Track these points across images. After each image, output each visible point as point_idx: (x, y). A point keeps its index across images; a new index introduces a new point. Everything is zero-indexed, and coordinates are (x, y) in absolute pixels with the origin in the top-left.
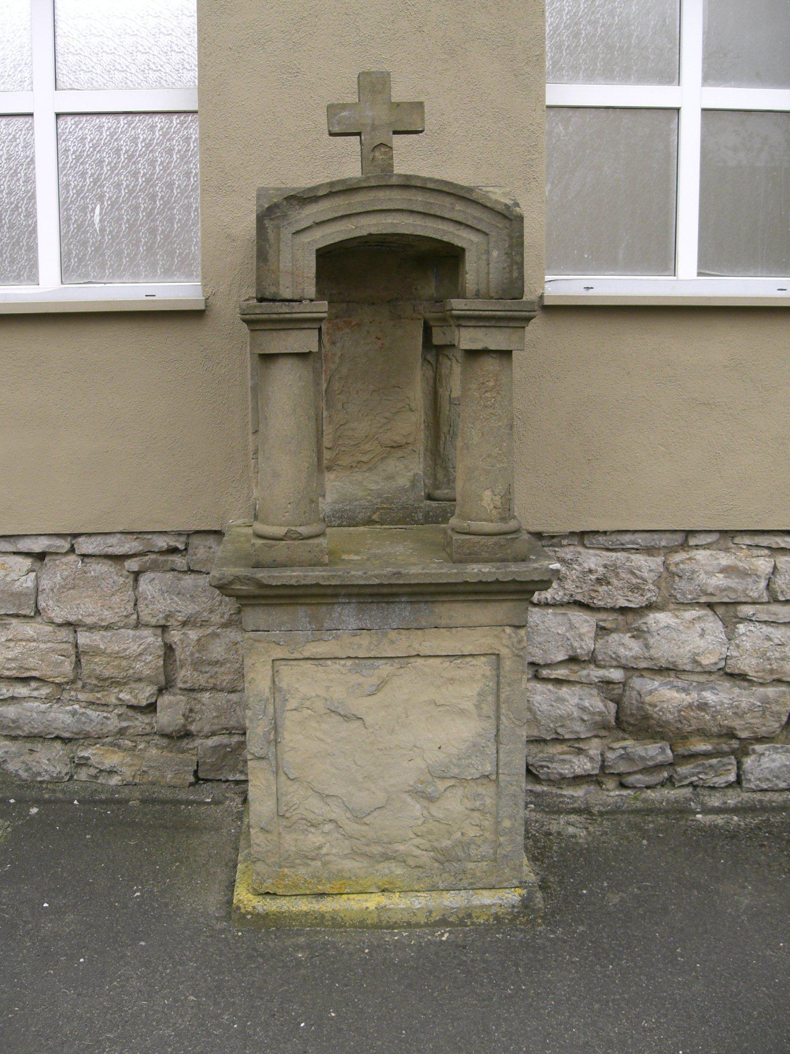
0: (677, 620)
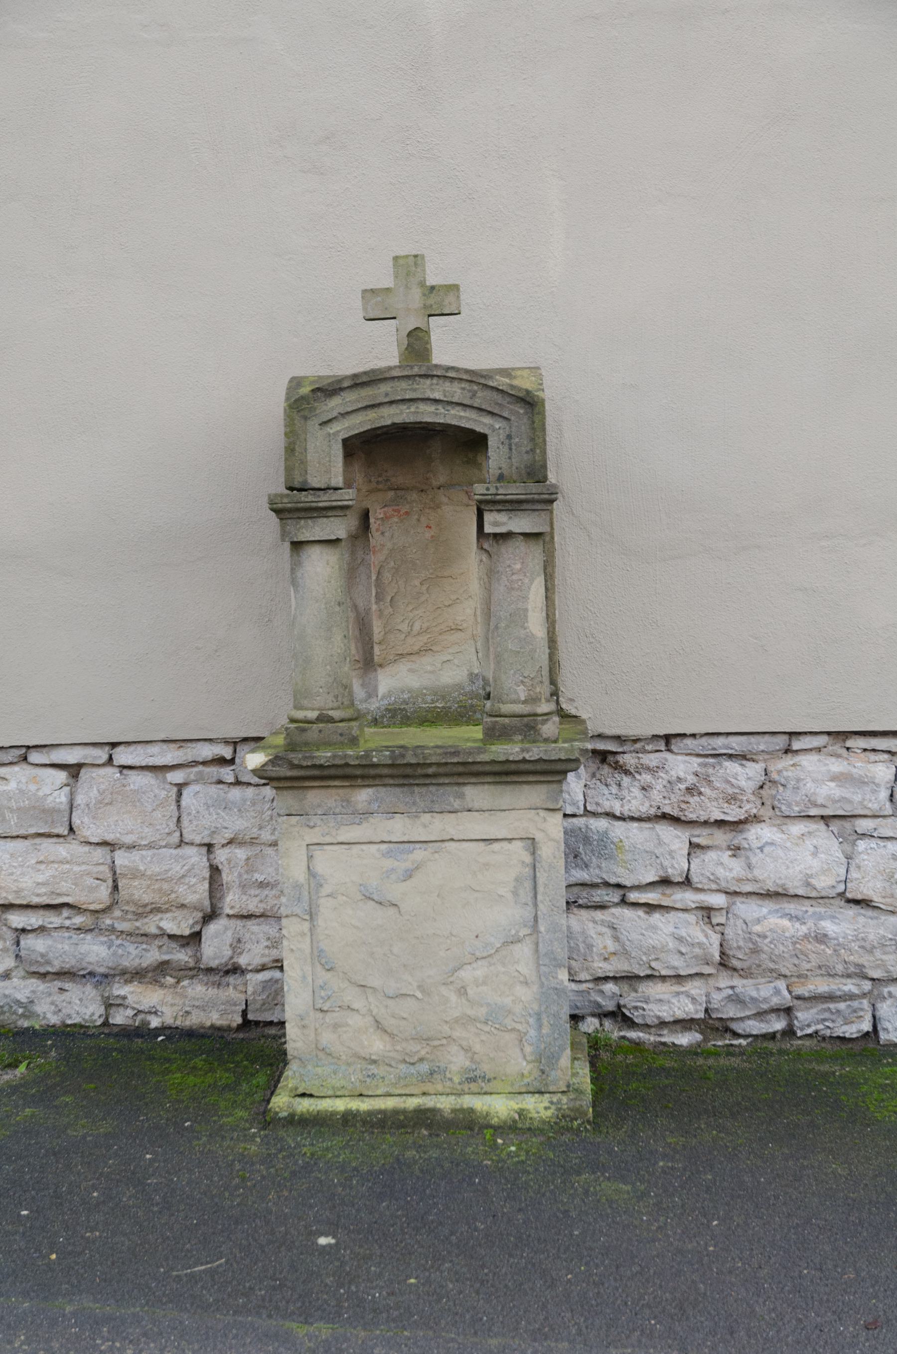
0: (783, 836)
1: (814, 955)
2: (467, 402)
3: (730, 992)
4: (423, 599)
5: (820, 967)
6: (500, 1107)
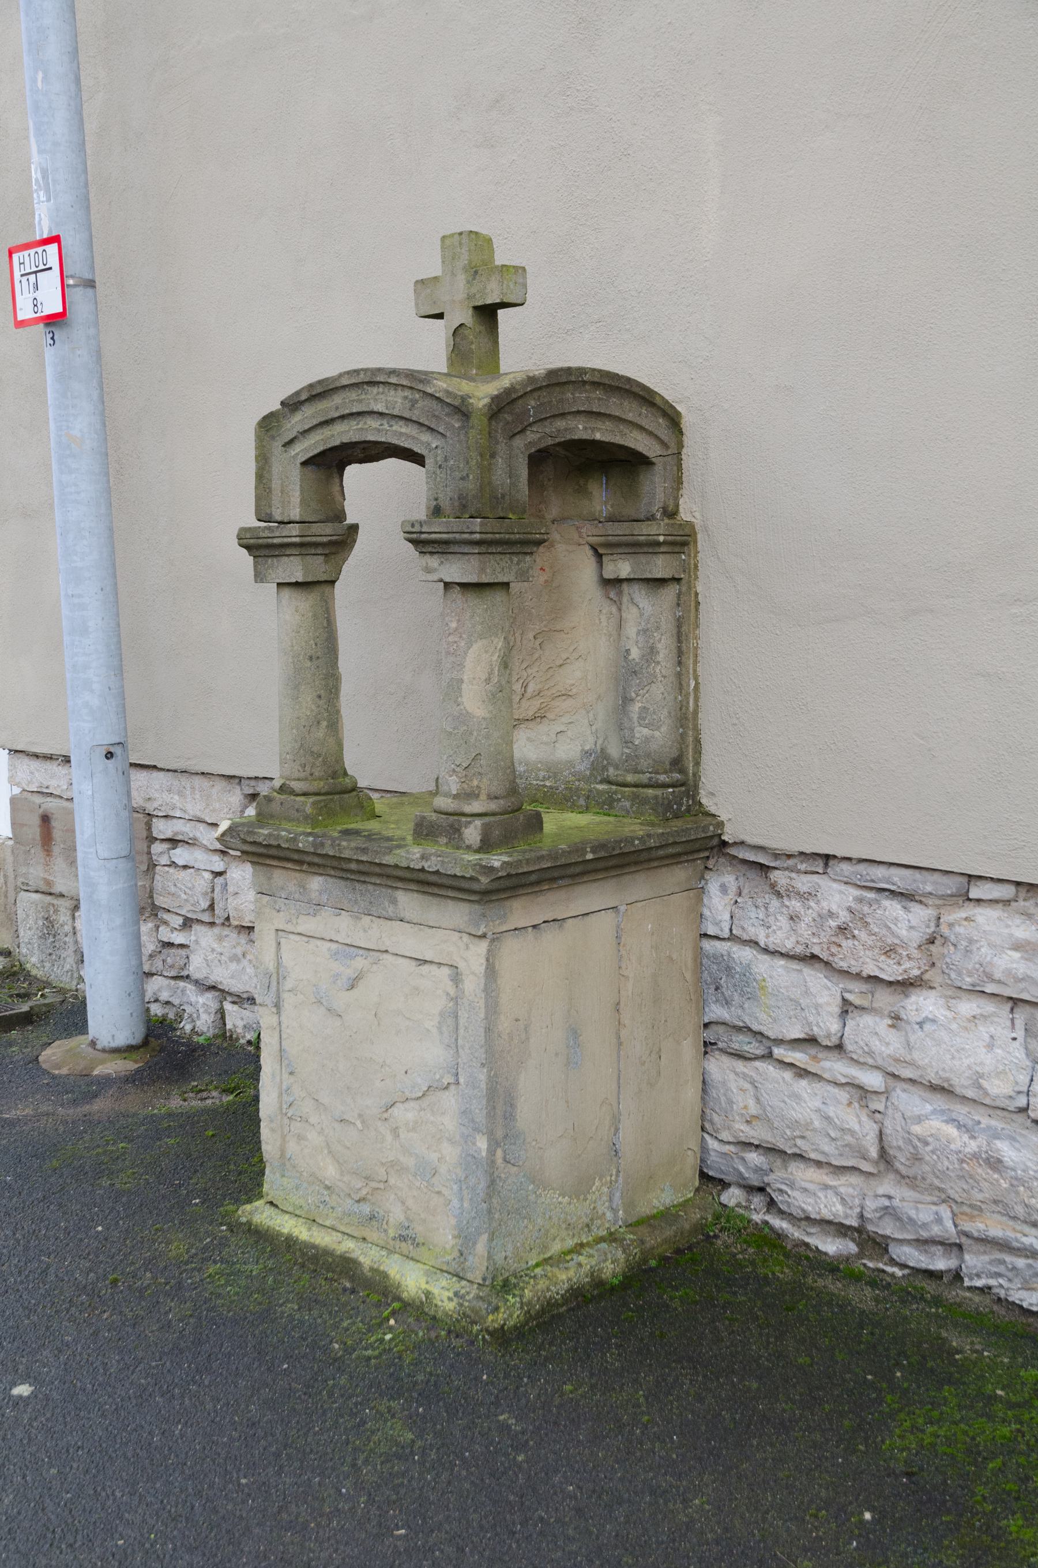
0: (948, 1013)
1: (987, 1184)
2: (406, 415)
3: (887, 1203)
4: (536, 656)
5: (996, 1202)
6: (411, 1279)
